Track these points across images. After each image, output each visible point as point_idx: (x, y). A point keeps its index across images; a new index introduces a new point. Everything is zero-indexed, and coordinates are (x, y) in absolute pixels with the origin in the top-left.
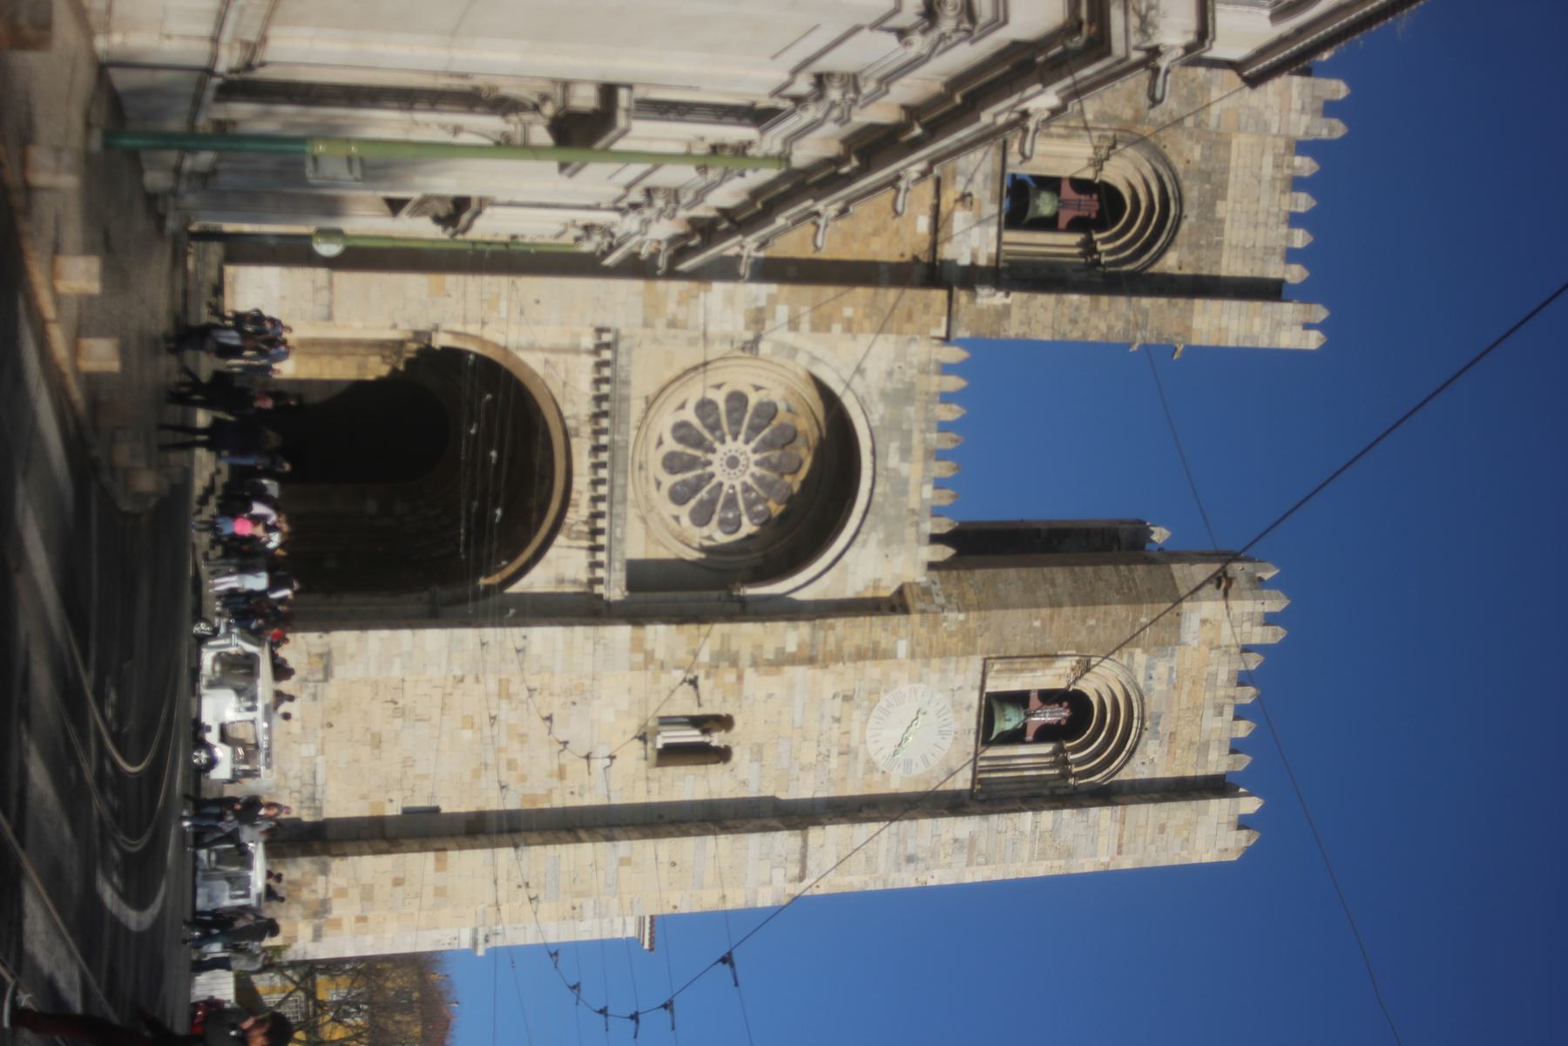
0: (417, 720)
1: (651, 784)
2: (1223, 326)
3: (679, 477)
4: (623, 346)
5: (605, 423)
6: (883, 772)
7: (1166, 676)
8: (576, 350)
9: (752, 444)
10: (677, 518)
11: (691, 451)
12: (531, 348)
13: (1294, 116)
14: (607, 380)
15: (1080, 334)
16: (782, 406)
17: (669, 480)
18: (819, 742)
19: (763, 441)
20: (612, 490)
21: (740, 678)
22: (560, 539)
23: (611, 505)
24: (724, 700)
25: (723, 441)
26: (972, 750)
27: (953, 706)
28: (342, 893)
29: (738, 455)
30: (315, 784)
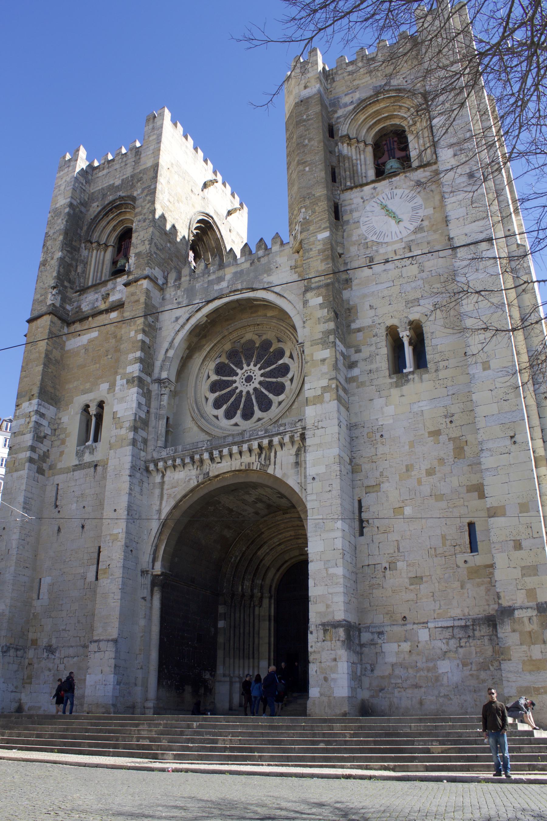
0: (399, 551)
1: (441, 367)
2: (152, 152)
3: (256, 408)
4: (156, 455)
5: (197, 457)
6: (422, 220)
7: (351, 95)
8: (162, 483)
9: (239, 371)
10: (280, 403)
11: (242, 406)
12: (159, 511)
13: (71, 168)
14: (175, 461)
15: (151, 214)
16: (218, 361)
17: (258, 413)
18: (403, 267)
19: (236, 366)
20: (234, 444)
21: (359, 330)
22: (270, 471)
23: (243, 442)
24: (376, 335)
25: (237, 388)
26: (402, 177)
27: (374, 197)
28: (531, 593)
29: (244, 378)
30: (453, 627)
